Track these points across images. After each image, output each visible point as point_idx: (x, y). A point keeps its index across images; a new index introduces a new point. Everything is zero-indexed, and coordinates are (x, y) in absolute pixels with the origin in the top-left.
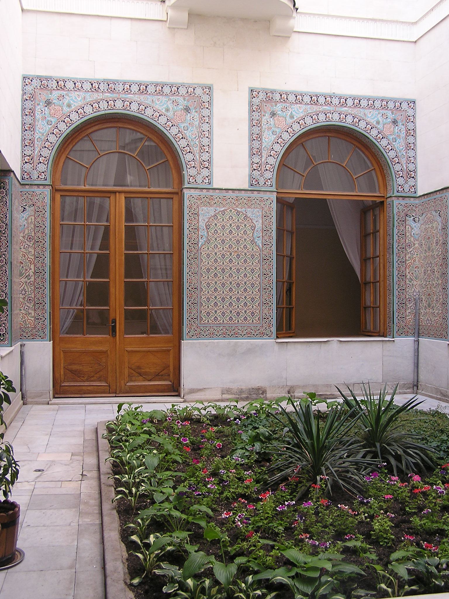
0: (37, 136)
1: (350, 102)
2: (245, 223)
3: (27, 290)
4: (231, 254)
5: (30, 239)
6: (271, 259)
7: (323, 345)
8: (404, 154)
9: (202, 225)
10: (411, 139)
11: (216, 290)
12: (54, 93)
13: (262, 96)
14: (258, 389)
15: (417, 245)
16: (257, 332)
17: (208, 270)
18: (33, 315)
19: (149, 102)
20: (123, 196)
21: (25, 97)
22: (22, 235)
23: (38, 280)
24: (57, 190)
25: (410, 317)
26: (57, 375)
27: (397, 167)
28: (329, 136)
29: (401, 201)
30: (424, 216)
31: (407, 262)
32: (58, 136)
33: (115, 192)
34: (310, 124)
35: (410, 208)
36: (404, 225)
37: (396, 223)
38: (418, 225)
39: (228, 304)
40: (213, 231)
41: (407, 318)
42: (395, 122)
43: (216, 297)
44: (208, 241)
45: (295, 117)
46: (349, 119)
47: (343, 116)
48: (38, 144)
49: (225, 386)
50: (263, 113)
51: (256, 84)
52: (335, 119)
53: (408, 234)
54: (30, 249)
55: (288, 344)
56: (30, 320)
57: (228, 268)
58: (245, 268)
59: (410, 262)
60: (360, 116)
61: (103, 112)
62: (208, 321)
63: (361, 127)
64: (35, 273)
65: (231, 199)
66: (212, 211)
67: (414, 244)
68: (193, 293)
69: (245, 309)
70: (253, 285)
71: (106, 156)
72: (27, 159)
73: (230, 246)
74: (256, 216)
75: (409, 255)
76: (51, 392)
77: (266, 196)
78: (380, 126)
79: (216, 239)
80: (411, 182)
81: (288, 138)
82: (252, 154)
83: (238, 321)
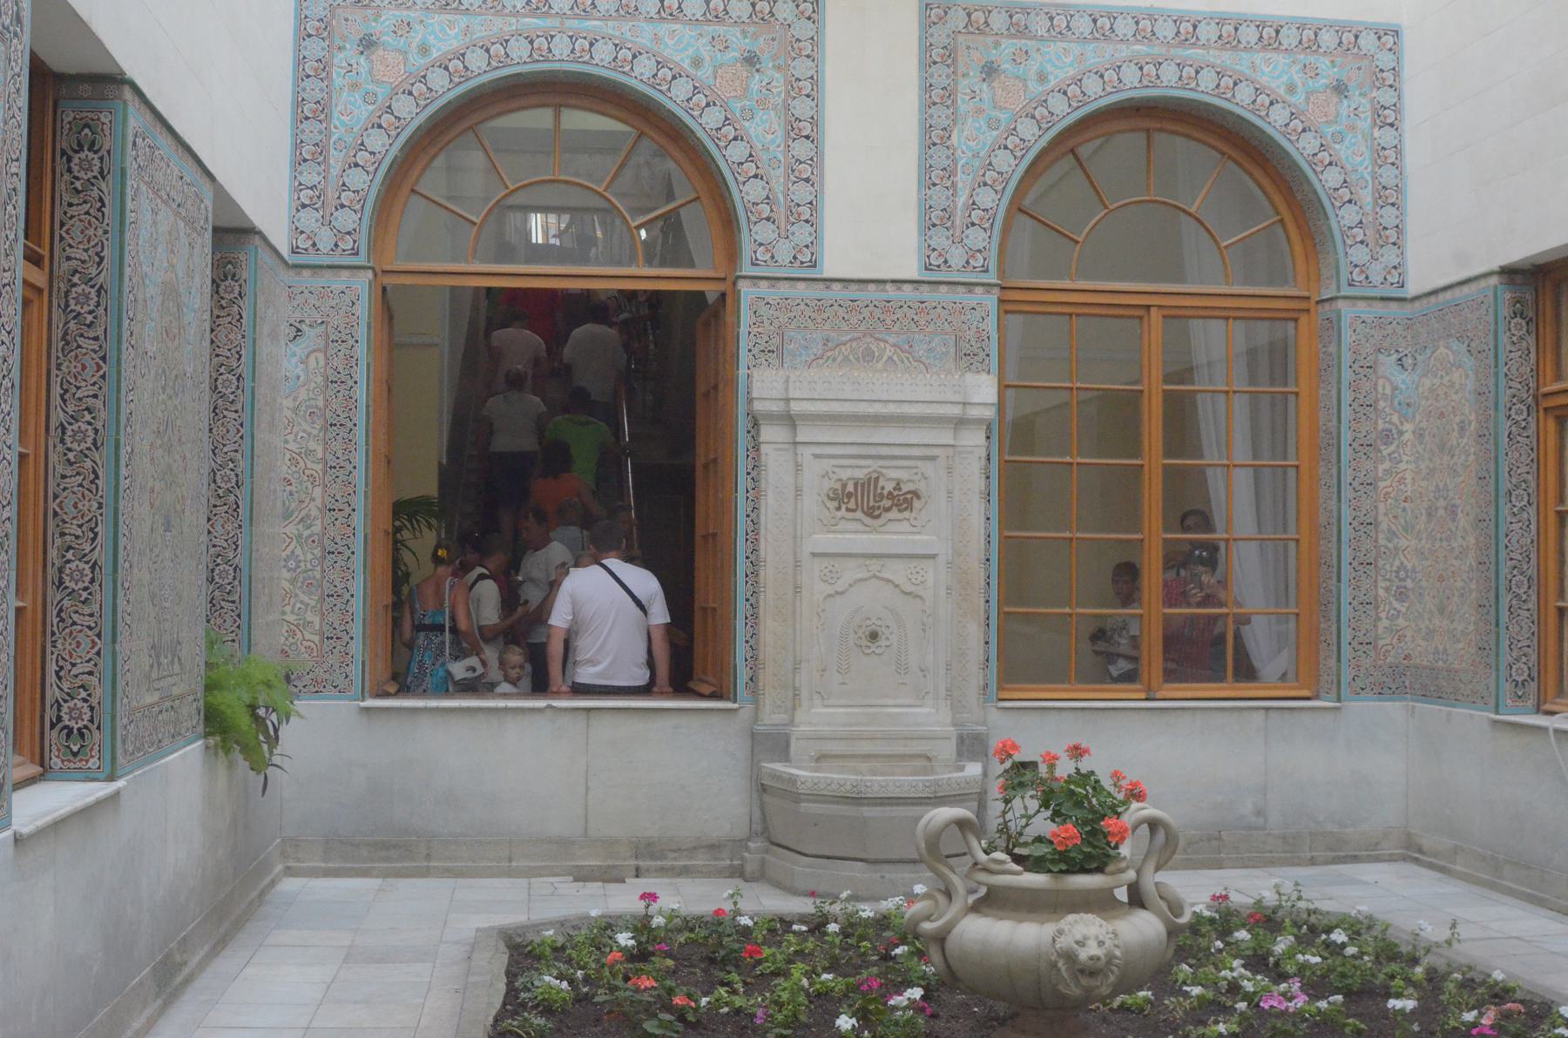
1: (1207, 32)
10: (1386, 136)
15: (1407, 436)
19: (645, 40)
22: (288, 403)
27: (1349, 215)
30: (1428, 352)
32: (393, 133)
34: (1098, 95)
42: (1340, 89)
45: (1051, 77)
46: (1207, 80)
47: (1189, 71)
48: (336, 159)
50: (961, 69)
52: (1169, 83)
53: (1382, 404)
54: (312, 445)
63: (1241, 102)
67: (1401, 433)
72: (305, 197)
75: (1387, 465)
78: (1298, 99)
80: (1390, 256)
81: (1034, 137)
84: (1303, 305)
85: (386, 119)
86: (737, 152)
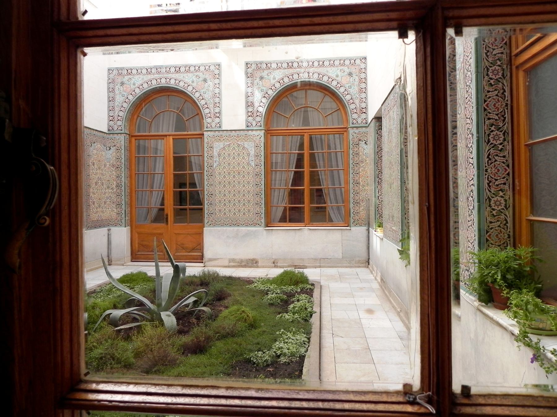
0: (116, 104)
1: (316, 64)
5: (113, 166)
7: (297, 231)
9: (215, 154)
10: (363, 85)
12: (126, 77)
13: (254, 66)
14: (253, 260)
15: (368, 161)
16: (252, 223)
20: (171, 138)
22: (108, 164)
24: (132, 136)
26: (134, 248)
27: (353, 106)
28: (306, 89)
33: (166, 136)
35: (362, 135)
37: (351, 146)
38: (368, 146)
42: (350, 74)
44: (220, 165)
48: (117, 109)
51: (250, 59)
53: (360, 154)
56: (114, 215)
63: (325, 81)
67: (366, 161)
71: (161, 114)
73: (234, 167)
75: (362, 168)
76: (130, 258)
78: (339, 79)
80: (363, 116)
86: (203, 102)
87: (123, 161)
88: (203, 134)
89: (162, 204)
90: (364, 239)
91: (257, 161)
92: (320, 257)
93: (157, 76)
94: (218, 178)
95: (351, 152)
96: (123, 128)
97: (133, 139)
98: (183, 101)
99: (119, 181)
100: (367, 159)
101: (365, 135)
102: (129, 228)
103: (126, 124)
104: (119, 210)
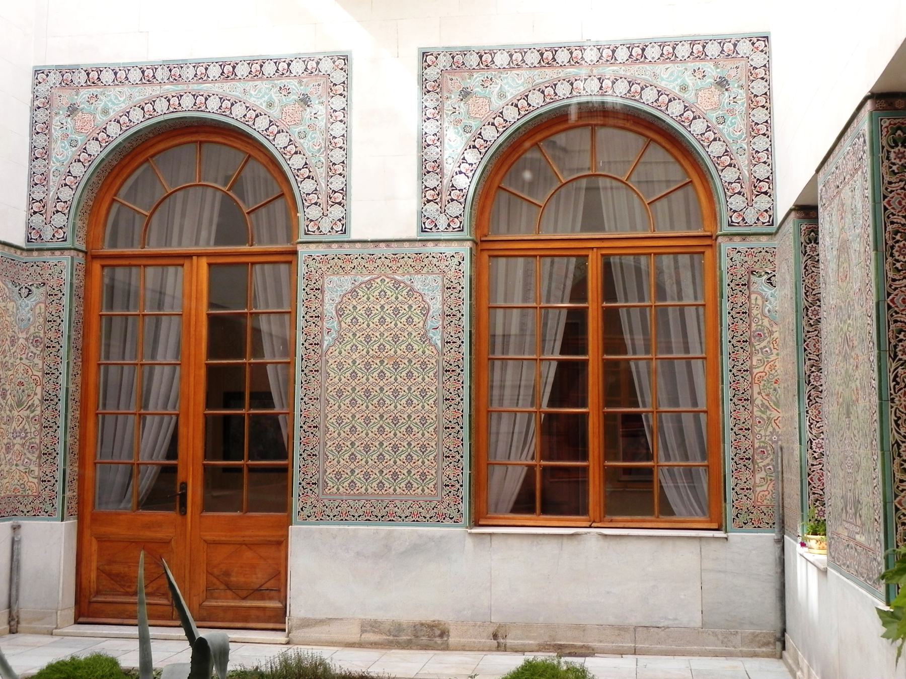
0: (53, 166)
1: (622, 54)
2: (410, 302)
3: (28, 430)
4: (382, 362)
5: (36, 342)
6: (458, 371)
7: (565, 541)
8: (745, 146)
9: (329, 308)
10: (760, 115)
11: (353, 429)
14: (432, 626)
15: (776, 335)
16: (432, 513)
17: (340, 393)
18: (36, 474)
20: (204, 262)
21: (36, 103)
23: (47, 414)
25: (765, 488)
26: (85, 582)
27: (729, 175)
29: (738, 243)
31: (755, 371)
32: (87, 165)
33: (189, 256)
36: (747, 292)
37: (726, 291)
38: (776, 291)
39: (375, 457)
40: (349, 320)
41: (758, 489)
42: (722, 83)
43: (353, 444)
44: (340, 339)
45: (508, 94)
48: (54, 181)
49: (369, 617)
50: (446, 94)
51: (433, 42)
53: (754, 312)
54: (36, 361)
55: (494, 538)
56: (32, 483)
57: (377, 389)
58: (410, 389)
59: (761, 369)
60: (644, 79)
61: (161, 118)
62: (338, 489)
63: (647, 101)
64: (44, 400)
65: (383, 259)
66: (346, 282)
67: (771, 333)
68: (312, 436)
69: (409, 467)
70: (424, 421)
72: (36, 207)
73: (382, 348)
74: (430, 288)
76: (71, 613)
77: (448, 249)
78: (689, 96)
79: (354, 335)
80: (762, 202)
82: (424, 173)
83: (395, 490)
84: (708, 242)
85: (83, 156)
87: (65, 327)
88: (295, 253)
89: (172, 452)
90: (769, 569)
91: (450, 329)
92: (634, 619)
93: (170, 89)
94: (335, 379)
95: (726, 306)
96: (68, 230)
97: (96, 266)
98: (242, 157)
99: (49, 387)
100: (775, 328)
101: (768, 256)
102: (72, 522)
103: (79, 223)
104: (47, 468)
